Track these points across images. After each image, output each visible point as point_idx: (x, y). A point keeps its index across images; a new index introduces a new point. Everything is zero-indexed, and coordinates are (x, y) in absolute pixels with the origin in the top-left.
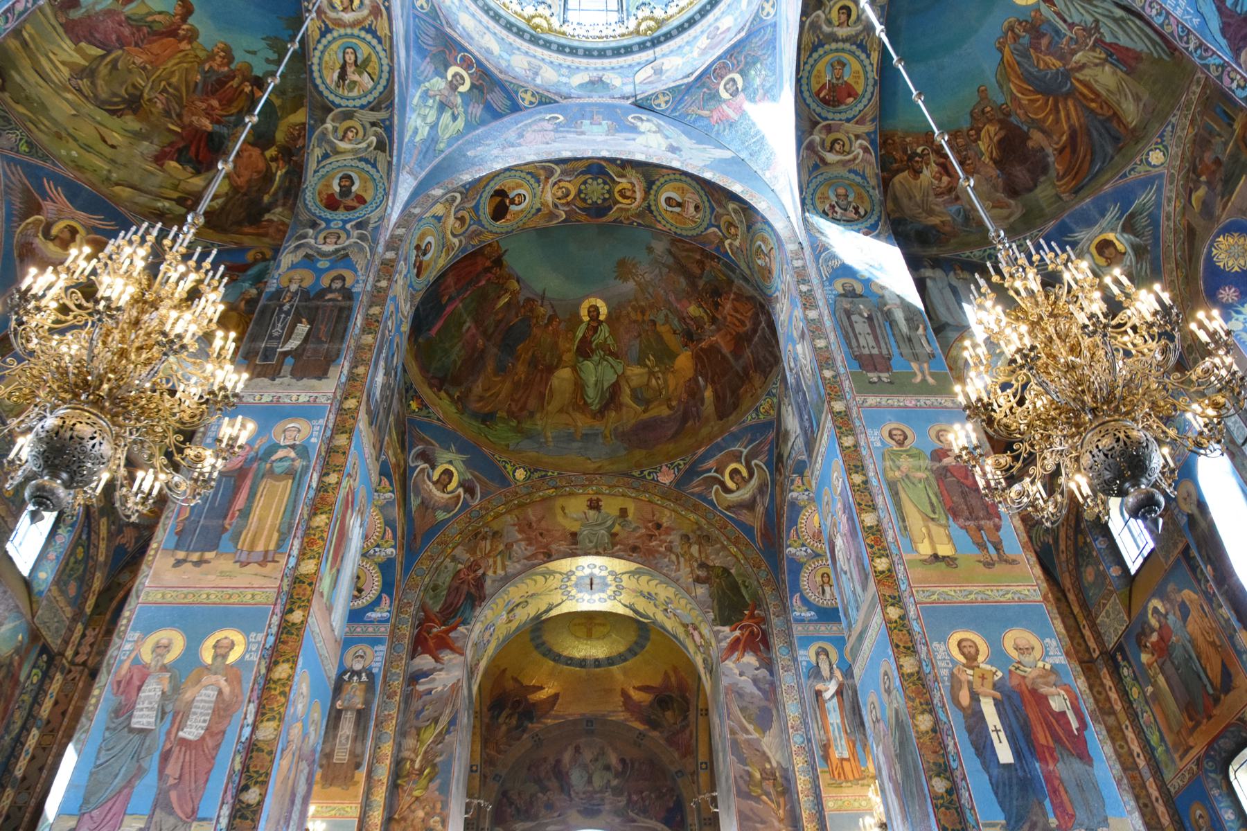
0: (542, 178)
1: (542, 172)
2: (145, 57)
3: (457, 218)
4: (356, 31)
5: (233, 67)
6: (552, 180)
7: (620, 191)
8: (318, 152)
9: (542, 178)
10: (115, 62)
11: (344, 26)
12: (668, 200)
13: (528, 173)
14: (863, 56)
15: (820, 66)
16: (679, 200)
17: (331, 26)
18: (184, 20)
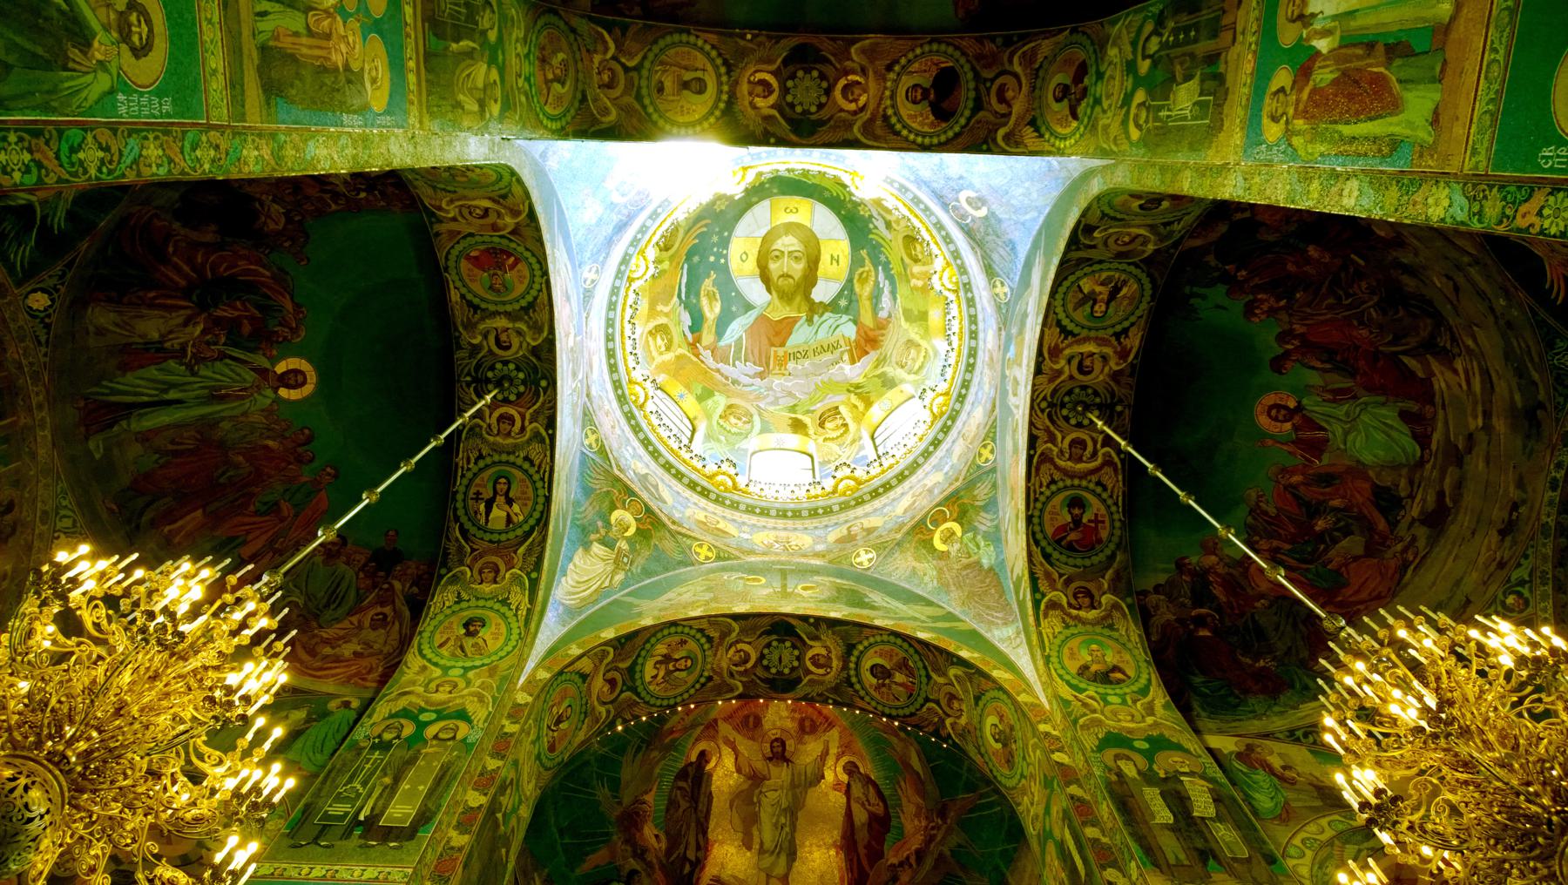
0: (879, 123)
1: (879, 132)
2: (1355, 333)
3: (1010, 105)
4: (1085, 333)
5: (1251, 297)
6: (866, 116)
7: (771, 92)
8: (1176, 227)
9: (879, 123)
10: (1390, 344)
11: (1096, 339)
12: (701, 92)
13: (897, 134)
14: (469, 297)
15: (521, 288)
16: (685, 92)
17: (1113, 339)
18: (1287, 354)
